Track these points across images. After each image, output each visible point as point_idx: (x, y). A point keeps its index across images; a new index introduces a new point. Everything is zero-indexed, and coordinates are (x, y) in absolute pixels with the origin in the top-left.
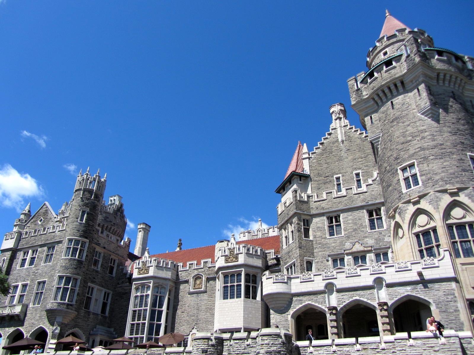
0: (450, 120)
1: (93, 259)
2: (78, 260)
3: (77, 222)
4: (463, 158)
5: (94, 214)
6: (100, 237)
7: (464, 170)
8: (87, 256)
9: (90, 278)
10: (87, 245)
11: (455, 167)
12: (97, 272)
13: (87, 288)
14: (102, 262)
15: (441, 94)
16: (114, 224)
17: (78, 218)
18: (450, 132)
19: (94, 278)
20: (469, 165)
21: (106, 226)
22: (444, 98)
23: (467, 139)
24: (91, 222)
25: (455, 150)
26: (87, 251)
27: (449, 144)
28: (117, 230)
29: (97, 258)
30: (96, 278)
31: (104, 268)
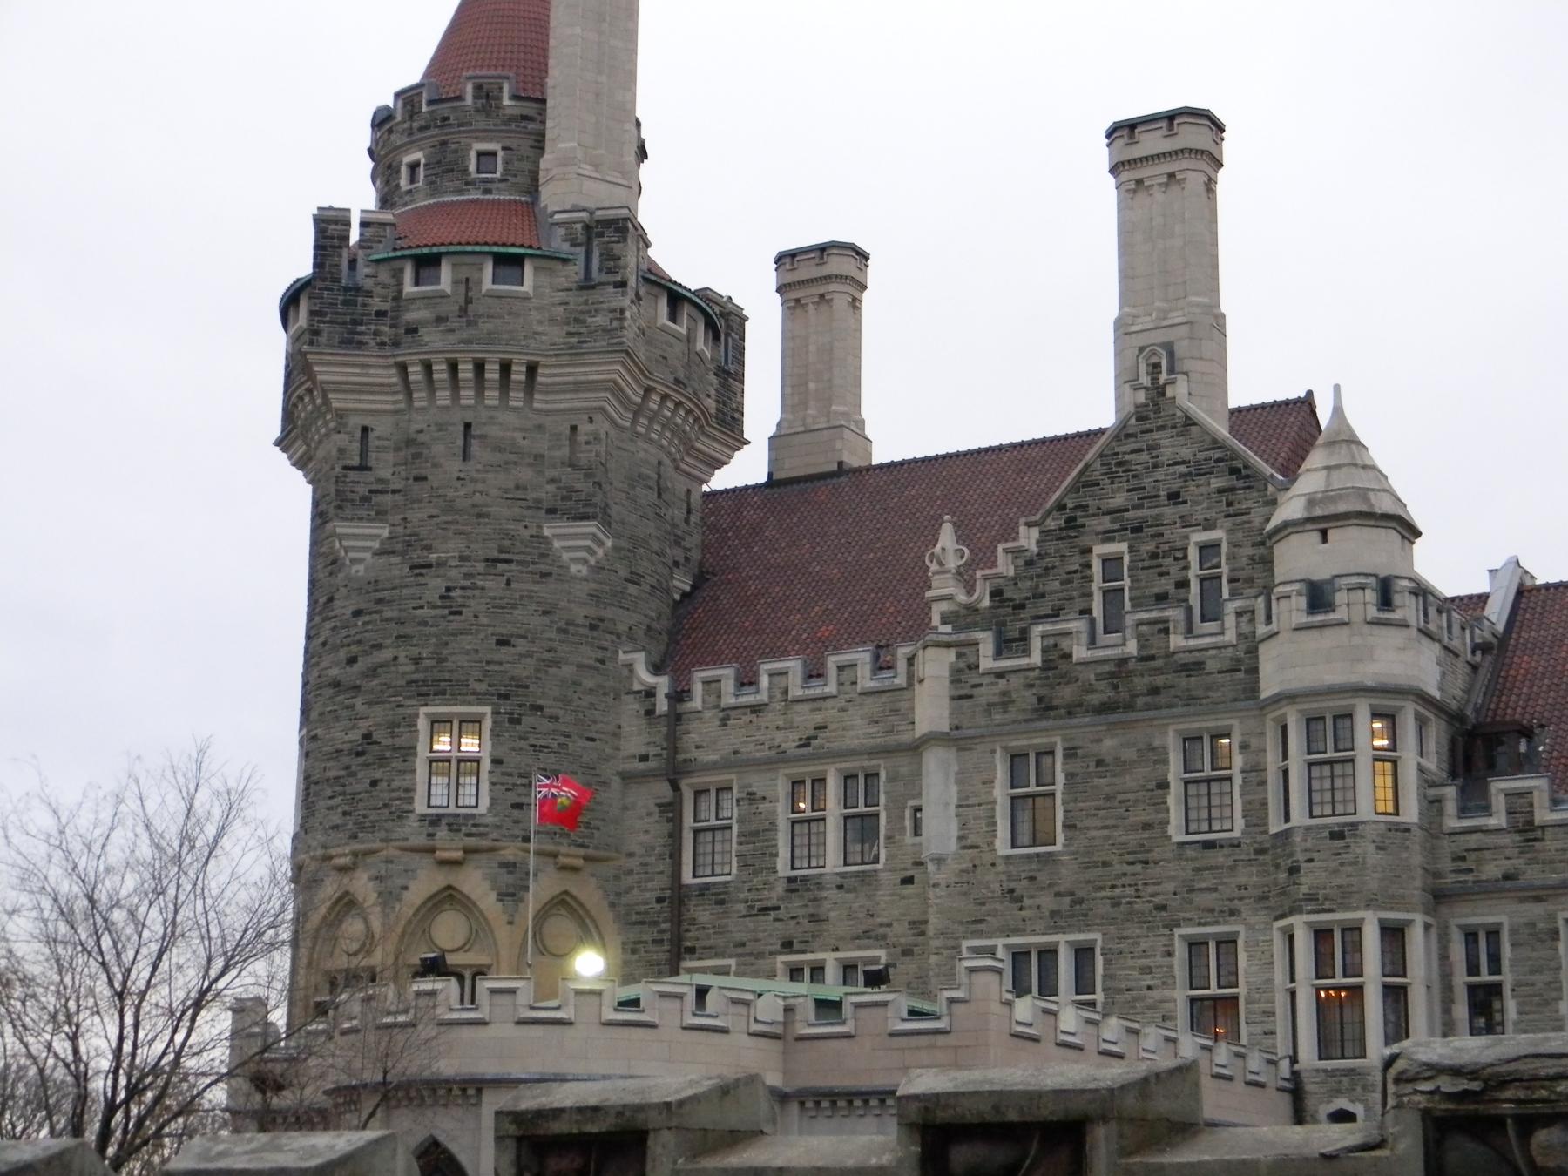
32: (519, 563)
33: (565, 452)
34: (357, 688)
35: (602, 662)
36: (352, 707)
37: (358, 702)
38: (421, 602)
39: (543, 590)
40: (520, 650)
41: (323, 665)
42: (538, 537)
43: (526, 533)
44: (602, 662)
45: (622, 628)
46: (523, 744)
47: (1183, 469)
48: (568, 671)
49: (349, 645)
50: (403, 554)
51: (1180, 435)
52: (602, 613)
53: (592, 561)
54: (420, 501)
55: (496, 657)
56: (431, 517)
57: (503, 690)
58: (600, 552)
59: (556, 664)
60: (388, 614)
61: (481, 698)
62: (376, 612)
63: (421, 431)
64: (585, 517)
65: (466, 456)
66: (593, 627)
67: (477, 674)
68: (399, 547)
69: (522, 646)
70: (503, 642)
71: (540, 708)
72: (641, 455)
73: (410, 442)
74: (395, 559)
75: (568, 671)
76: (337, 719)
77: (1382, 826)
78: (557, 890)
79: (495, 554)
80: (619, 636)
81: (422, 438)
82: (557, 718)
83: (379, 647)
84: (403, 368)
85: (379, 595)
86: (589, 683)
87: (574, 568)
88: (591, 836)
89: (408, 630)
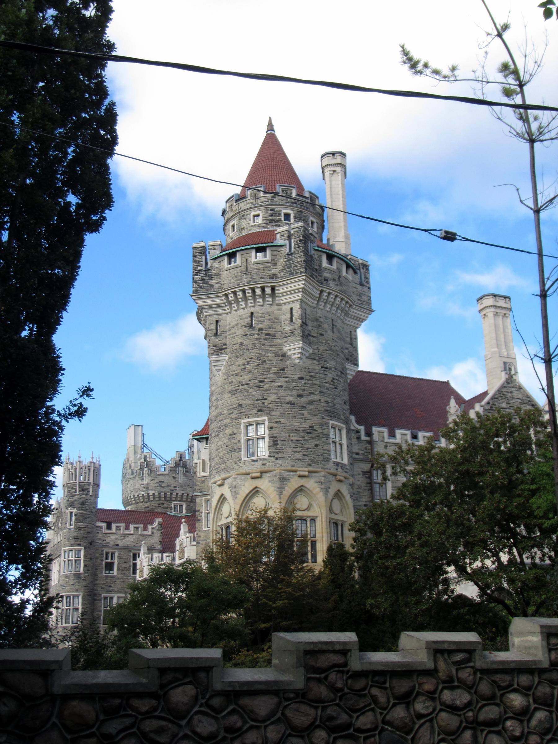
0: (234, 371)
1: (102, 564)
2: (75, 575)
3: (66, 528)
4: (235, 431)
5: (84, 512)
6: (106, 534)
7: (232, 451)
8: (85, 566)
9: (103, 588)
10: (83, 552)
11: (225, 447)
12: (113, 577)
13: (101, 600)
14: (118, 564)
15: (233, 327)
16: (175, 487)
17: (66, 524)
18: (230, 392)
19: (110, 586)
20: (239, 441)
21: (163, 494)
22: (235, 333)
23: (248, 395)
24: (82, 524)
25: (229, 420)
26: (84, 561)
27: (226, 412)
28: (183, 494)
29: (110, 561)
30: (113, 585)
31: (123, 570)
34: (305, 407)
36: (303, 414)
37: (306, 413)
38: (327, 381)
41: (280, 395)
47: (520, 401)
49: (298, 390)
50: (318, 361)
51: (518, 391)
54: (322, 343)
56: (326, 350)
60: (315, 382)
62: (311, 380)
63: (320, 317)
68: (317, 358)
73: (317, 320)
74: (317, 362)
76: (295, 417)
81: (321, 320)
83: (313, 394)
84: (322, 292)
85: (311, 374)
89: (323, 390)
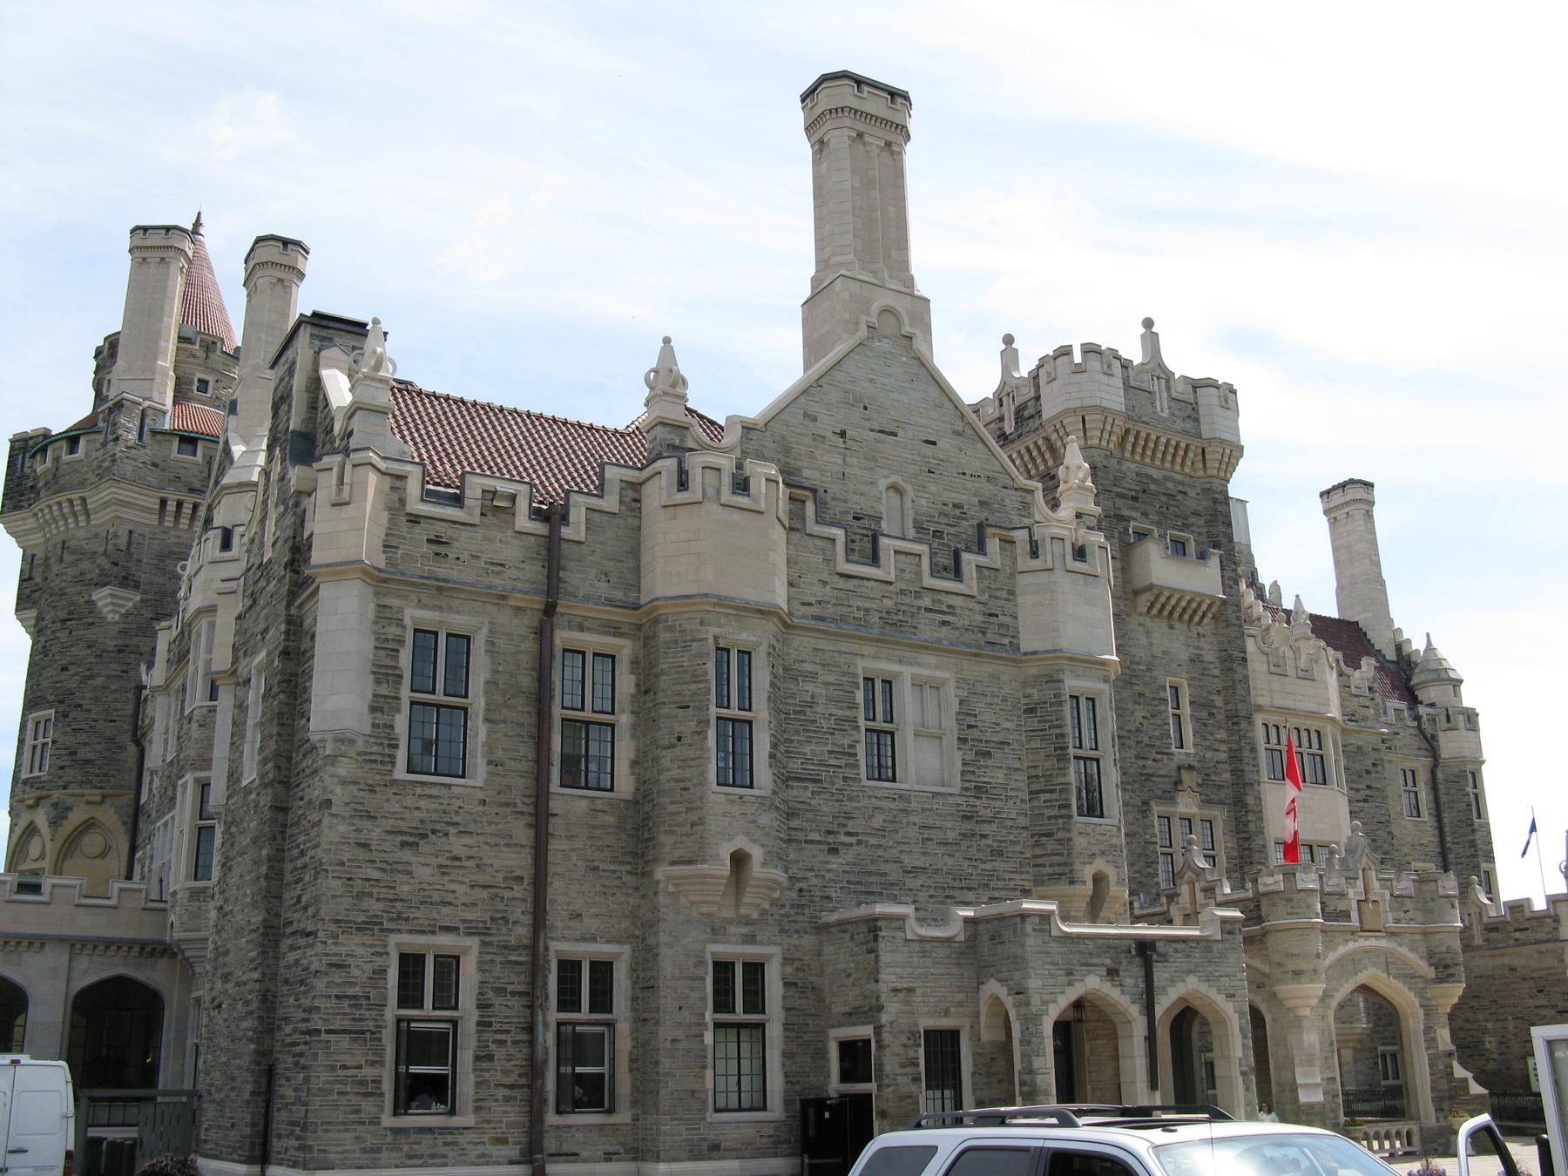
32: (80, 619)
33: (102, 549)
35: (126, 672)
39: (89, 634)
40: (72, 672)
42: (90, 603)
43: (82, 601)
44: (126, 672)
45: (143, 649)
46: (68, 729)
48: (99, 681)
52: (128, 642)
53: (123, 611)
55: (63, 678)
57: (61, 698)
58: (130, 604)
59: (92, 677)
61: (50, 705)
64: (105, 585)
65: (61, 560)
66: (120, 651)
67: (50, 691)
69: (73, 669)
70: (64, 669)
71: (80, 706)
72: (174, 540)
75: (99, 681)
77: (205, 710)
78: (85, 818)
79: (66, 616)
80: (141, 654)
82: (89, 711)
86: (114, 687)
87: (110, 617)
88: (109, 781)
